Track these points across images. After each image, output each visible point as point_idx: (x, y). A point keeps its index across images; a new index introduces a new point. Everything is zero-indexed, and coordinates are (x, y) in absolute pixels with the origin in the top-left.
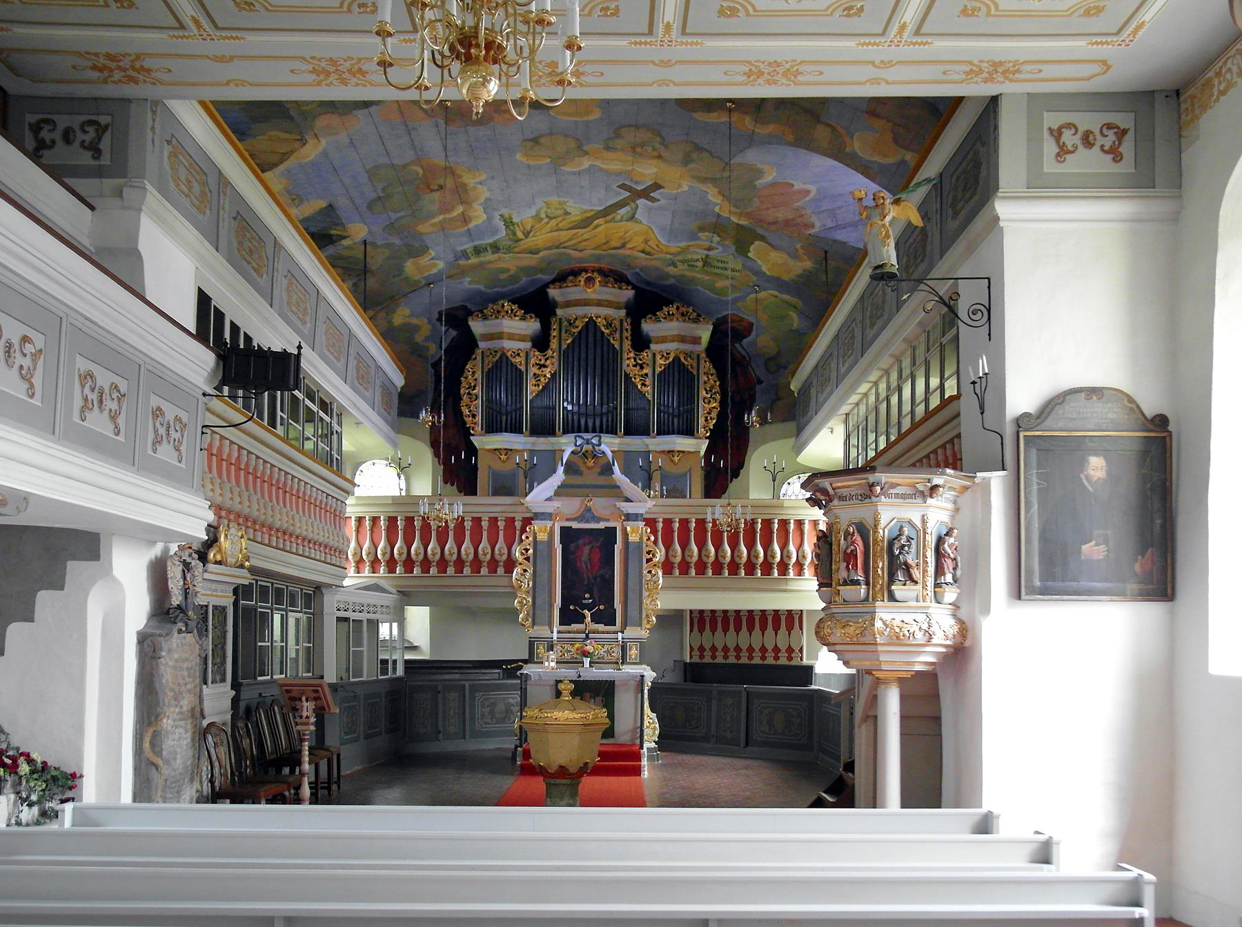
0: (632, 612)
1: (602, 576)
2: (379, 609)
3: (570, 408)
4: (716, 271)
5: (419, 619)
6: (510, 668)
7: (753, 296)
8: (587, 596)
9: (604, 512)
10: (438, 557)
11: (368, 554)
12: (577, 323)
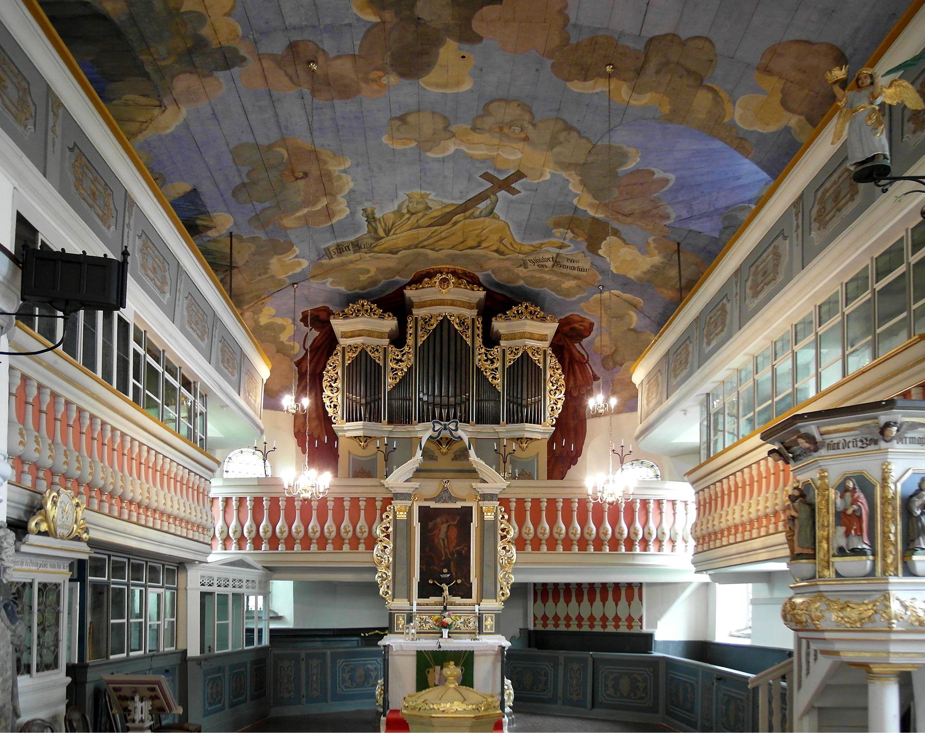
0: (488, 584)
1: (459, 553)
2: (244, 584)
3: (425, 398)
4: (564, 271)
5: (283, 595)
6: (371, 637)
7: (598, 296)
8: (445, 571)
9: (462, 492)
10: (302, 534)
11: (235, 532)
12: (432, 321)
